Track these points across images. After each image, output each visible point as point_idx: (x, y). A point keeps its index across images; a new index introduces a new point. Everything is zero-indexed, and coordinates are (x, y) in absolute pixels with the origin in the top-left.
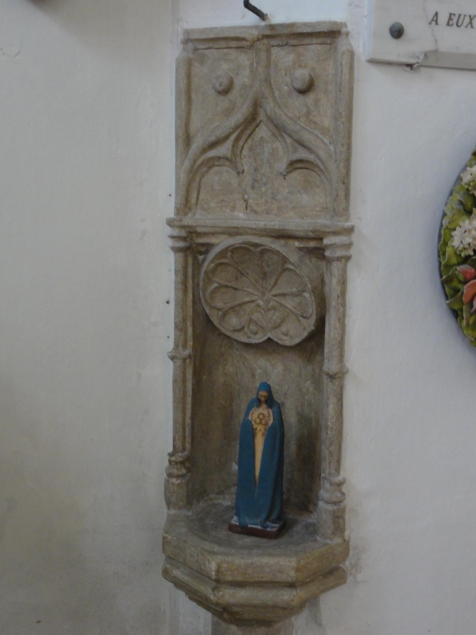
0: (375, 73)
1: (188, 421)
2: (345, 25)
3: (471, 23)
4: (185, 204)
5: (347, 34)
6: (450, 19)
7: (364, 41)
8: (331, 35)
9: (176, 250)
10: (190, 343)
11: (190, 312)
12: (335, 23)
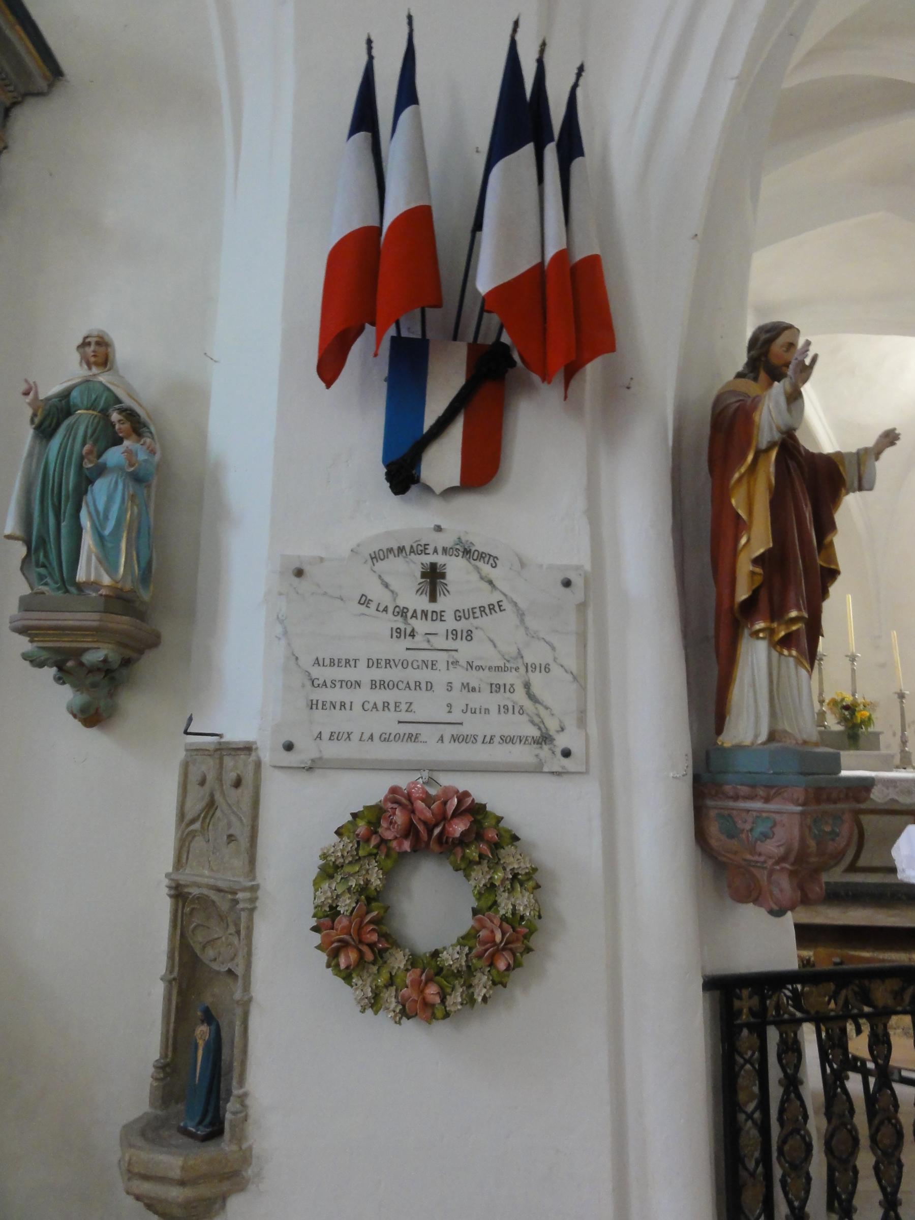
0: (278, 773)
1: (171, 1033)
2: (255, 743)
3: (349, 737)
4: (179, 864)
5: (257, 749)
6: (331, 735)
7: (268, 754)
8: (248, 749)
9: (171, 896)
10: (176, 969)
11: (177, 944)
12: (248, 742)
